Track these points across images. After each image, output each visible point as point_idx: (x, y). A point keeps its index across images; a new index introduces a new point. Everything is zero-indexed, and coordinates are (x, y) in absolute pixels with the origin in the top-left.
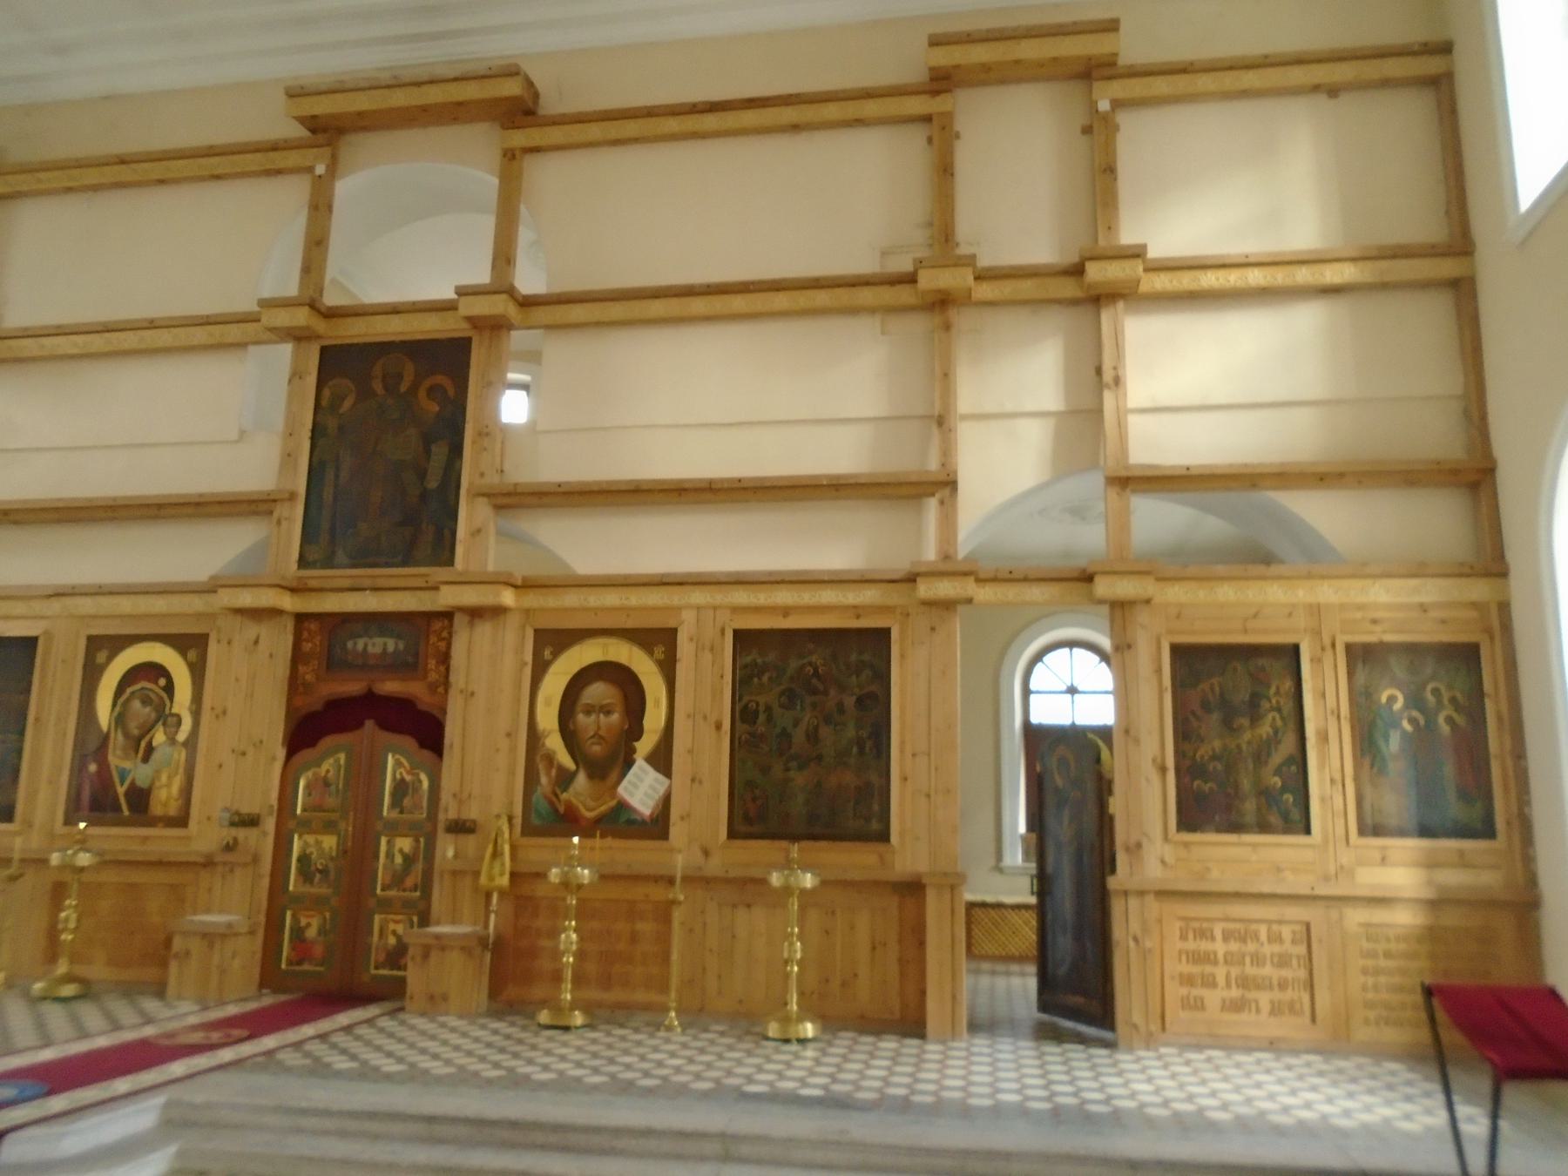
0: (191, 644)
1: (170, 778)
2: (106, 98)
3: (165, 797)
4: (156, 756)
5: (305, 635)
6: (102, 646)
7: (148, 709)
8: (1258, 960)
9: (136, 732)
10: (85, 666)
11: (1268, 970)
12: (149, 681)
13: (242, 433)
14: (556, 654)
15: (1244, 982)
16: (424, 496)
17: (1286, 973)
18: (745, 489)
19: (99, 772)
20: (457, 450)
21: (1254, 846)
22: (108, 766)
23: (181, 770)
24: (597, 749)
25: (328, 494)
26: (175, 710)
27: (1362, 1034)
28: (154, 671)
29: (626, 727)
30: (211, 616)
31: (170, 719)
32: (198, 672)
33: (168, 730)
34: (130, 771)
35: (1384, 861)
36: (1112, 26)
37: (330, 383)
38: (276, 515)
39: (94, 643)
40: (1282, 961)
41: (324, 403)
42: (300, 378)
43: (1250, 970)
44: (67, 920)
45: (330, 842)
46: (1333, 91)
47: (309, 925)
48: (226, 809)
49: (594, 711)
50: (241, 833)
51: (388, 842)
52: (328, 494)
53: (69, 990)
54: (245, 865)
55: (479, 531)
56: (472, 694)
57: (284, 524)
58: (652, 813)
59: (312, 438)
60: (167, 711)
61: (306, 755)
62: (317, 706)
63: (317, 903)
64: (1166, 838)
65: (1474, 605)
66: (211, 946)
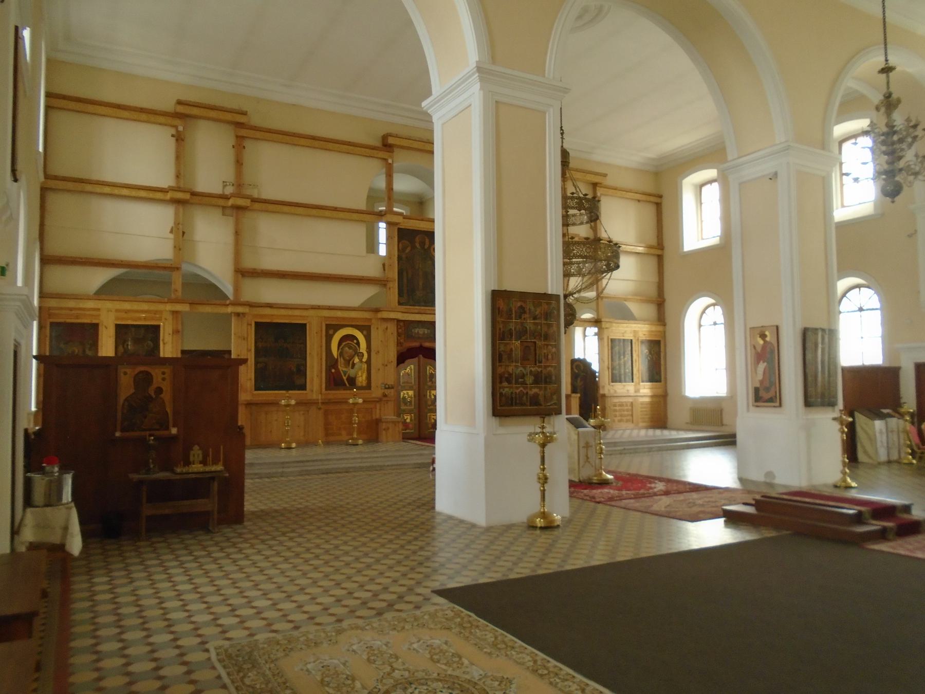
0: (366, 329)
1: (362, 374)
2: (294, 105)
3: (361, 379)
5: (399, 327)
6: (332, 328)
7: (351, 351)
8: (624, 411)
9: (348, 358)
11: (626, 413)
15: (621, 416)
17: (628, 413)
21: (624, 386)
23: (366, 371)
25: (405, 280)
26: (361, 351)
27: (641, 424)
28: (352, 337)
30: (370, 320)
31: (359, 354)
34: (347, 372)
35: (644, 388)
36: (605, 175)
38: (388, 287)
39: (328, 327)
40: (627, 410)
41: (400, 248)
42: (391, 238)
43: (623, 413)
44: (355, 420)
45: (411, 393)
46: (639, 201)
47: (407, 418)
48: (383, 384)
50: (389, 391)
51: (429, 392)
52: (405, 280)
53: (360, 442)
54: (390, 401)
61: (401, 365)
62: (405, 350)
63: (410, 412)
64: (609, 384)
65: (660, 331)
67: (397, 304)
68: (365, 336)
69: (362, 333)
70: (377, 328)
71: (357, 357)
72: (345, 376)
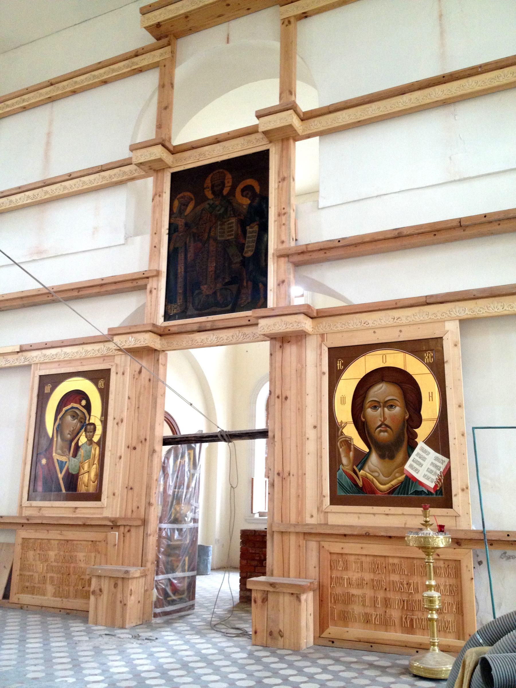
1: (89, 467)
4: (82, 452)
10: (38, 396)
12: (76, 403)
13: (126, 239)
14: (346, 365)
16: (244, 262)
18: (490, 222)
19: (47, 463)
20: (264, 228)
22: (53, 459)
23: (96, 462)
24: (384, 436)
25: (181, 269)
26: (91, 422)
29: (407, 417)
31: (89, 427)
32: (104, 394)
33: (88, 434)
34: (66, 462)
37: (179, 196)
38: (149, 287)
41: (175, 210)
42: (160, 196)
49: (380, 407)
52: (181, 269)
54: (138, 526)
55: (283, 282)
56: (286, 398)
57: (154, 292)
58: (436, 486)
59: (169, 234)
60: (87, 422)
66: (116, 585)
67: (162, 319)
68: (100, 391)
69: (96, 385)
70: (123, 374)
71: (84, 434)
72: (61, 473)
